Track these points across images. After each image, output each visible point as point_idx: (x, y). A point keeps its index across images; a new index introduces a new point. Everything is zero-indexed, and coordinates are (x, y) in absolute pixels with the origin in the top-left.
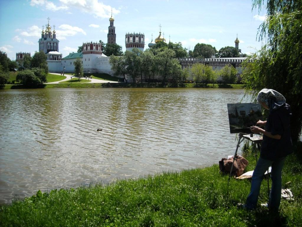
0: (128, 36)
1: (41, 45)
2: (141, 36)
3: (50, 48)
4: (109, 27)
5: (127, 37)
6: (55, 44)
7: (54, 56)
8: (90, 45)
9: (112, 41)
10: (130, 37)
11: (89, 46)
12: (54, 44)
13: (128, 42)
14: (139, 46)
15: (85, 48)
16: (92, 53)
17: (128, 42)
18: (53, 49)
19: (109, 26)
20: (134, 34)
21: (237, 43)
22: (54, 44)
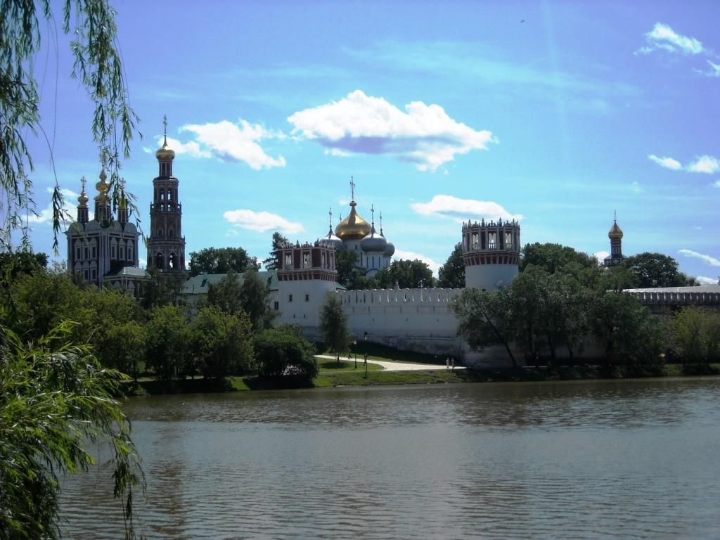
0: (469, 231)
1: (78, 243)
2: (513, 229)
3: (118, 257)
4: (158, 179)
5: (479, 231)
6: (130, 243)
7: (139, 285)
8: (311, 251)
9: (171, 228)
10: (489, 232)
11: (307, 253)
12: (126, 241)
13: (483, 247)
14: (511, 258)
15: (289, 261)
16: (317, 276)
17: (483, 247)
18: (124, 259)
19: (157, 175)
20: (500, 224)
21: (616, 237)
22: (126, 241)
